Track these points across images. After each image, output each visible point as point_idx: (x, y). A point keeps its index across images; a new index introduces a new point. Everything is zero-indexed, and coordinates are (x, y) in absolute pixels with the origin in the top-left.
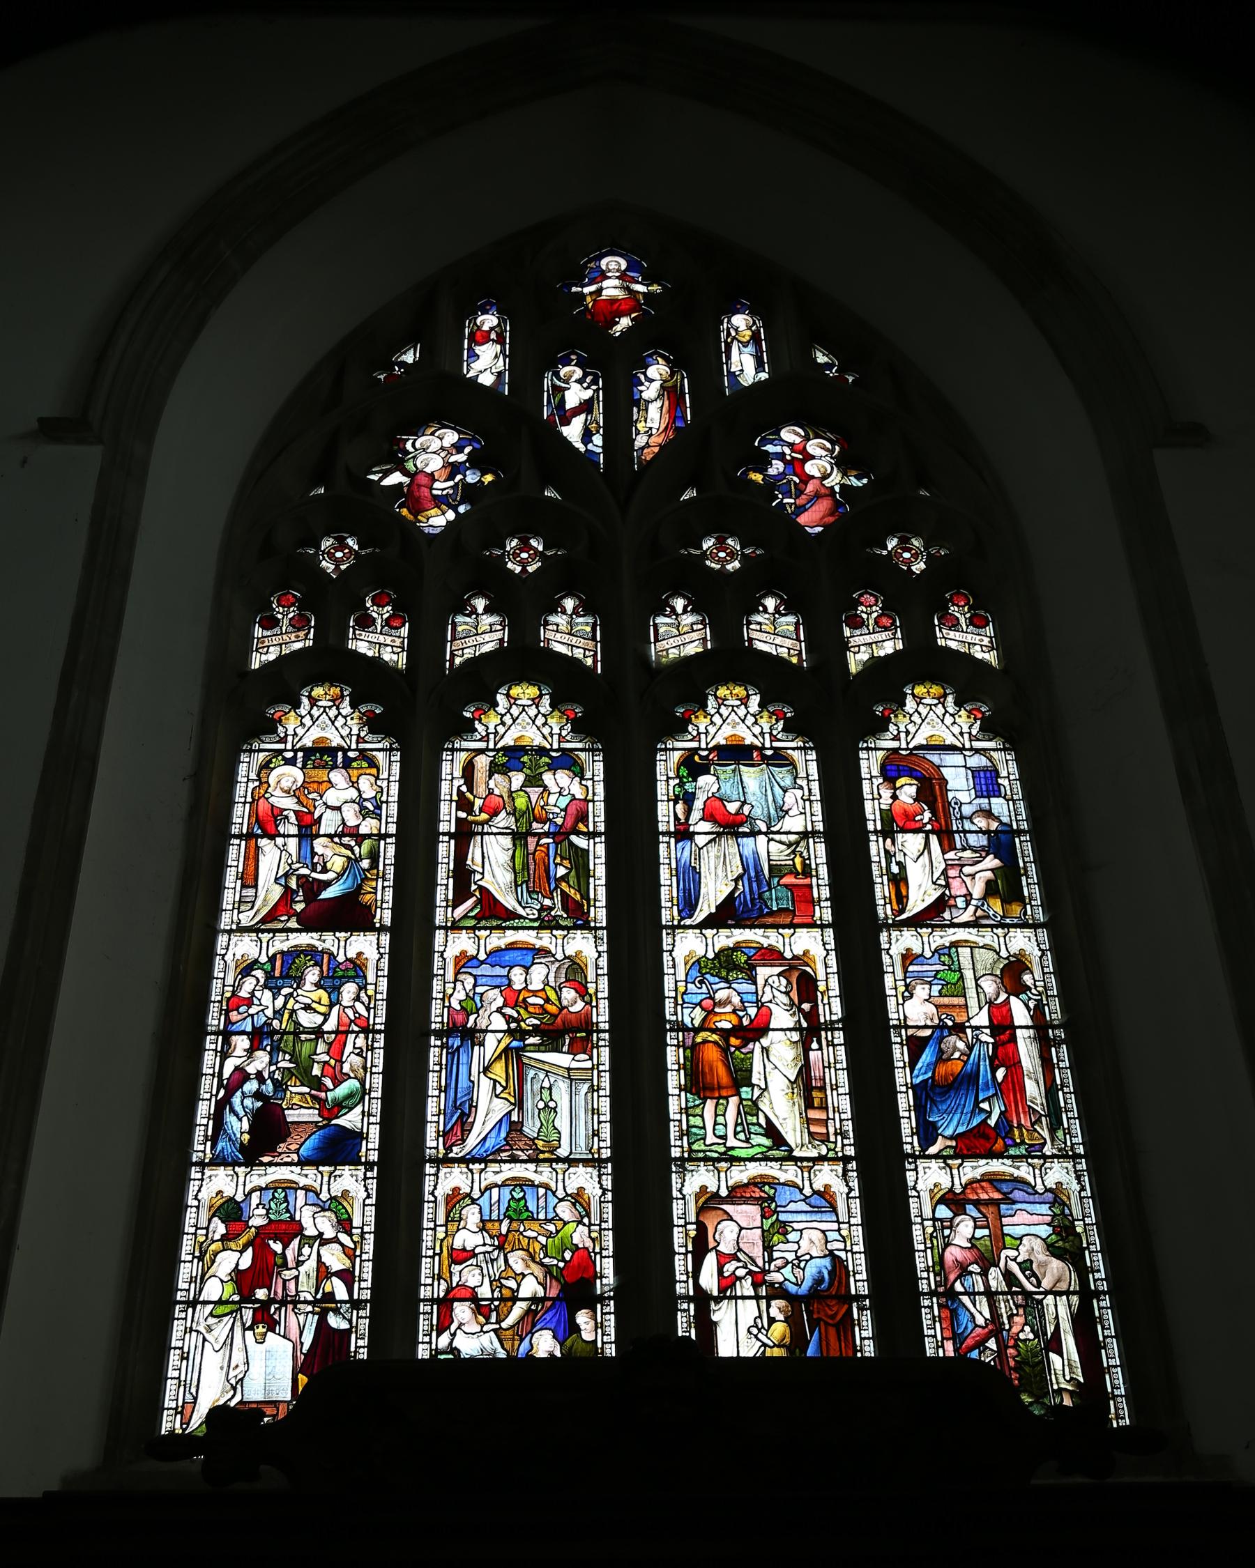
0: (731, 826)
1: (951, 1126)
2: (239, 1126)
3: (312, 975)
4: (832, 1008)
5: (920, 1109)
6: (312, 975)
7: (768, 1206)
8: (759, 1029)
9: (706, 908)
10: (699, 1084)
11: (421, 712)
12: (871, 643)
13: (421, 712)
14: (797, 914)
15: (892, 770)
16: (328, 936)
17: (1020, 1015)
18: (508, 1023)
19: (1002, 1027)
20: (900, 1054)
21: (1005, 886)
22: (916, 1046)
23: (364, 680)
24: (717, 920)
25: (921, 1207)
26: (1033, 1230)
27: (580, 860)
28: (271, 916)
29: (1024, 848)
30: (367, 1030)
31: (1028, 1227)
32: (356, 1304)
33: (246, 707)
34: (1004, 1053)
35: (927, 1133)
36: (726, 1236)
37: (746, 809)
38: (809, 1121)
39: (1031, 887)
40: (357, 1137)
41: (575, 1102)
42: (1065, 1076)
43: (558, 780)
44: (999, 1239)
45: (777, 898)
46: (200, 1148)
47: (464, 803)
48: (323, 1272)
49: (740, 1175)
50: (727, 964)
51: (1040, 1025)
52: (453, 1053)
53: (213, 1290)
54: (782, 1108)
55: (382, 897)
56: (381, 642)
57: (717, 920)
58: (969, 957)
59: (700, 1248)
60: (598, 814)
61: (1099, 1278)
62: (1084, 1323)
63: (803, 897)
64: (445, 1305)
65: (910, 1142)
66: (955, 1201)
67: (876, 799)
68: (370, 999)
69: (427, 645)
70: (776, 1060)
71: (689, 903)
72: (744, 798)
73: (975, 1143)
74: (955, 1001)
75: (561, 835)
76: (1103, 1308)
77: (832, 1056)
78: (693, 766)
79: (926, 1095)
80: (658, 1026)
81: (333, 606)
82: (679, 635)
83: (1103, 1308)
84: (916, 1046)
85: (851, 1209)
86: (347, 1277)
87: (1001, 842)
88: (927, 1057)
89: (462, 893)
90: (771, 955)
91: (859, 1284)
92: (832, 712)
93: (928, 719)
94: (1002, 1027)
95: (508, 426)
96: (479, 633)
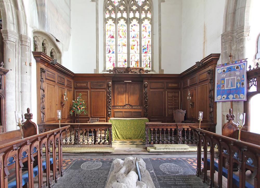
1: (144, 51)
3: (111, 41)
4: (139, 44)
6: (111, 41)
8: (134, 45)
9: (132, 37)
10: (132, 49)
11: (116, 21)
12: (143, 16)
13: (116, 21)
17: (149, 45)
19: (148, 45)
21: (149, 36)
24: (133, 37)
29: (150, 32)
31: (148, 58)
33: (106, 20)
34: (148, 47)
35: (143, 52)
41: (125, 49)
44: (146, 58)
45: (136, 36)
47: (119, 29)
57: (133, 37)
58: (146, 41)
61: (151, 61)
62: (150, 63)
63: (138, 36)
65: (142, 53)
67: (143, 29)
68: (114, 43)
70: (135, 47)
73: (146, 53)
75: (124, 31)
76: (151, 62)
77: (139, 47)
78: (132, 26)
82: (131, 15)
83: (151, 62)
84: (143, 46)
92: (140, 21)
93: (146, 23)
94: (148, 45)
96: (119, 15)
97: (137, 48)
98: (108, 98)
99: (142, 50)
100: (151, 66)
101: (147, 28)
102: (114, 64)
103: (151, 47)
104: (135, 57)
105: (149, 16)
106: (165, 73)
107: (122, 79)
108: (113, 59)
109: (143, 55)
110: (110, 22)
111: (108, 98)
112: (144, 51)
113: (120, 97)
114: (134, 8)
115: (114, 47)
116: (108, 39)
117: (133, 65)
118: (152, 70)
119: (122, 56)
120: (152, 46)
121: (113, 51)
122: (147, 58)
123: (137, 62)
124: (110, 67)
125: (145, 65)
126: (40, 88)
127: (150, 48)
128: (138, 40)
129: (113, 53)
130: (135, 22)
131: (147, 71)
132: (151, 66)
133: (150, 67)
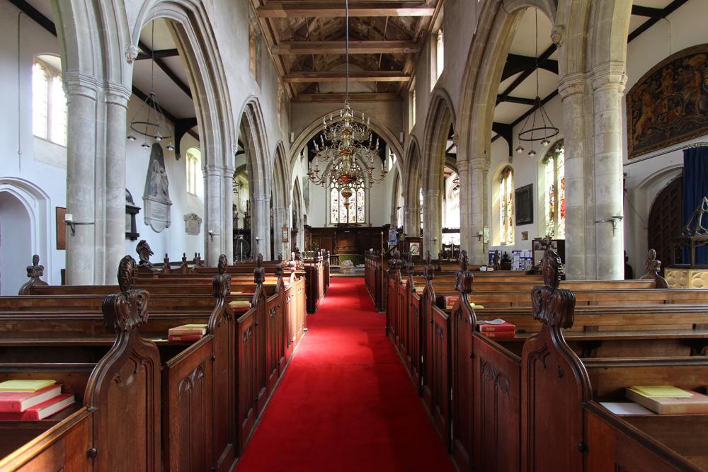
33: (331, 189)
58: (361, 202)
67: (358, 194)
68: (337, 205)
93: (361, 190)
97: (354, 207)
98: (333, 242)
99: (358, 209)
104: (352, 211)
105: (363, 185)
106: (373, 226)
107: (343, 230)
108: (337, 215)
109: (358, 212)
110: (335, 190)
111: (333, 242)
113: (341, 242)
115: (337, 207)
116: (333, 201)
117: (351, 221)
118: (365, 223)
120: (365, 206)
122: (361, 215)
124: (334, 221)
126: (305, 240)
127: (363, 208)
128: (355, 202)
131: (360, 224)
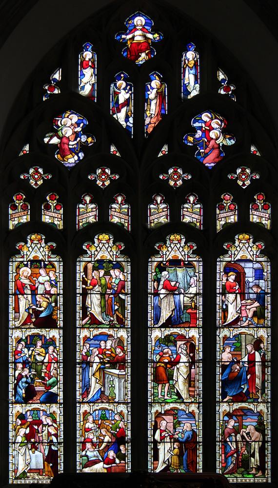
0: (172, 291)
1: (232, 393)
2: (22, 392)
3: (39, 343)
4: (200, 355)
5: (223, 387)
6: (39, 343)
7: (175, 416)
8: (177, 362)
9: (162, 321)
10: (157, 380)
11: (69, 244)
12: (227, 217)
13: (69, 244)
14: (190, 325)
15: (227, 271)
16: (43, 330)
17: (258, 358)
18: (100, 360)
19: (252, 361)
20: (218, 370)
21: (259, 314)
22: (224, 368)
23: (49, 232)
25: (220, 417)
26: (252, 423)
27: (122, 303)
28: (25, 323)
29: (268, 298)
30: (57, 362)
31: (250, 424)
32: (59, 443)
35: (224, 395)
36: (163, 425)
37: (177, 284)
38: (189, 391)
39: (268, 314)
40: (57, 395)
42: (268, 377)
43: (115, 273)
45: (185, 317)
46: (11, 398)
47: (84, 282)
48: (49, 434)
49: (168, 407)
50: (168, 340)
51: (263, 360)
52: (84, 370)
53: (19, 439)
54: (181, 386)
55: (60, 316)
56: (52, 217)
59: (155, 428)
60: (128, 285)
61: (269, 437)
62: (262, 450)
63: (194, 317)
64: (84, 444)
65: (218, 397)
66: (229, 415)
68: (57, 352)
69: (70, 217)
70: (181, 372)
71: (157, 319)
72: (178, 279)
73: (238, 398)
74: (238, 353)
75: (116, 294)
76: (268, 446)
77: (198, 371)
78: (161, 268)
79: (225, 384)
80: (146, 361)
81: (36, 201)
84: (224, 368)
85: (199, 418)
86: (56, 435)
87: (260, 298)
88: (227, 371)
89: (84, 316)
90: (182, 337)
91: (200, 439)
92: (209, 244)
93: (244, 249)
94: (252, 361)
95: (96, 113)
100: (269, 465)
101: (249, 273)
102: (51, 457)
103: (268, 371)
108: (52, 429)
112: (232, 393)
114: (176, 177)
115: (57, 372)
119: (104, 418)
121: (54, 390)
123: (187, 446)
125: (232, 460)
129: (51, 399)
130: (176, 248)
132: (269, 465)
133: (261, 468)
